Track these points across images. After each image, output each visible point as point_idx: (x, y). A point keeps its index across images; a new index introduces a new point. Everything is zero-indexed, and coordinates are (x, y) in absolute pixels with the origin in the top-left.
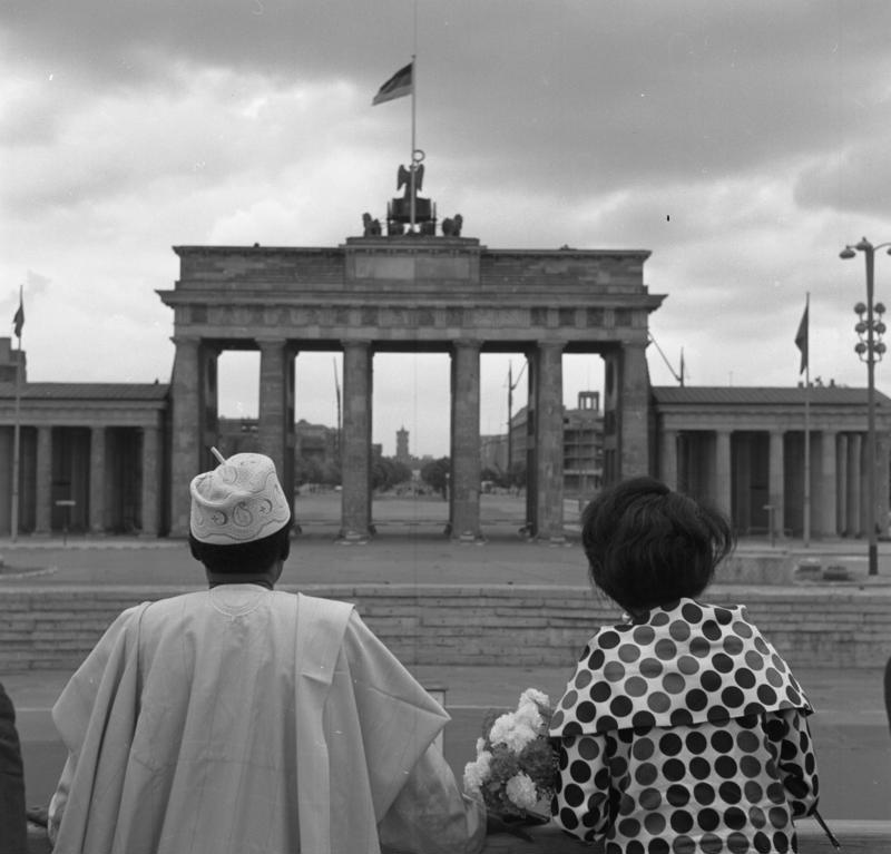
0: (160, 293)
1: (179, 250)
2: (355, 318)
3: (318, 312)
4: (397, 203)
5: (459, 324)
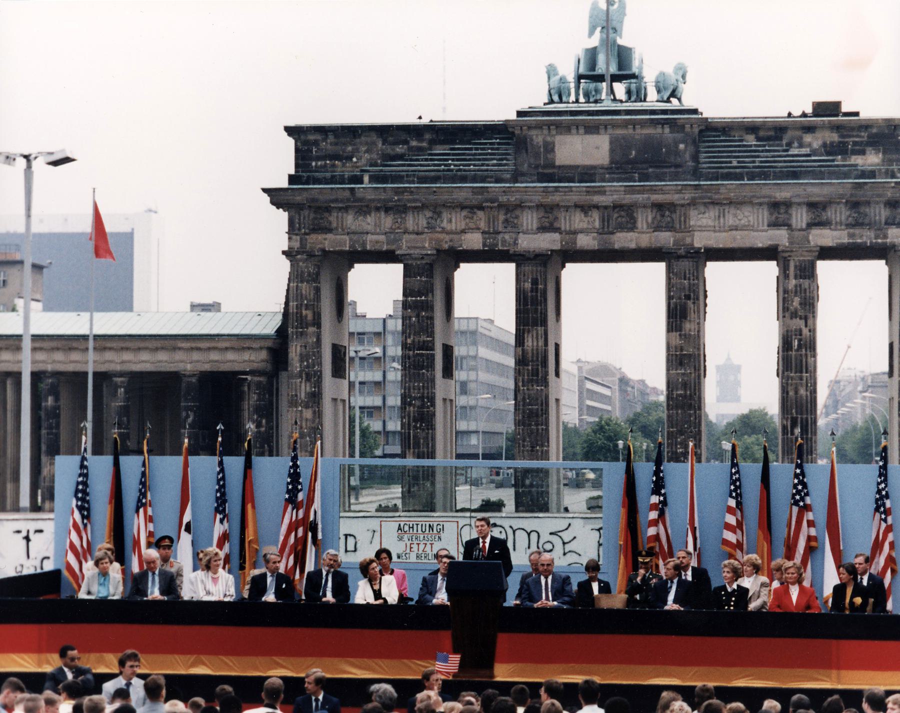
0: (265, 190)
1: (291, 131)
2: (529, 219)
3: (480, 214)
4: (592, 54)
5: (670, 228)
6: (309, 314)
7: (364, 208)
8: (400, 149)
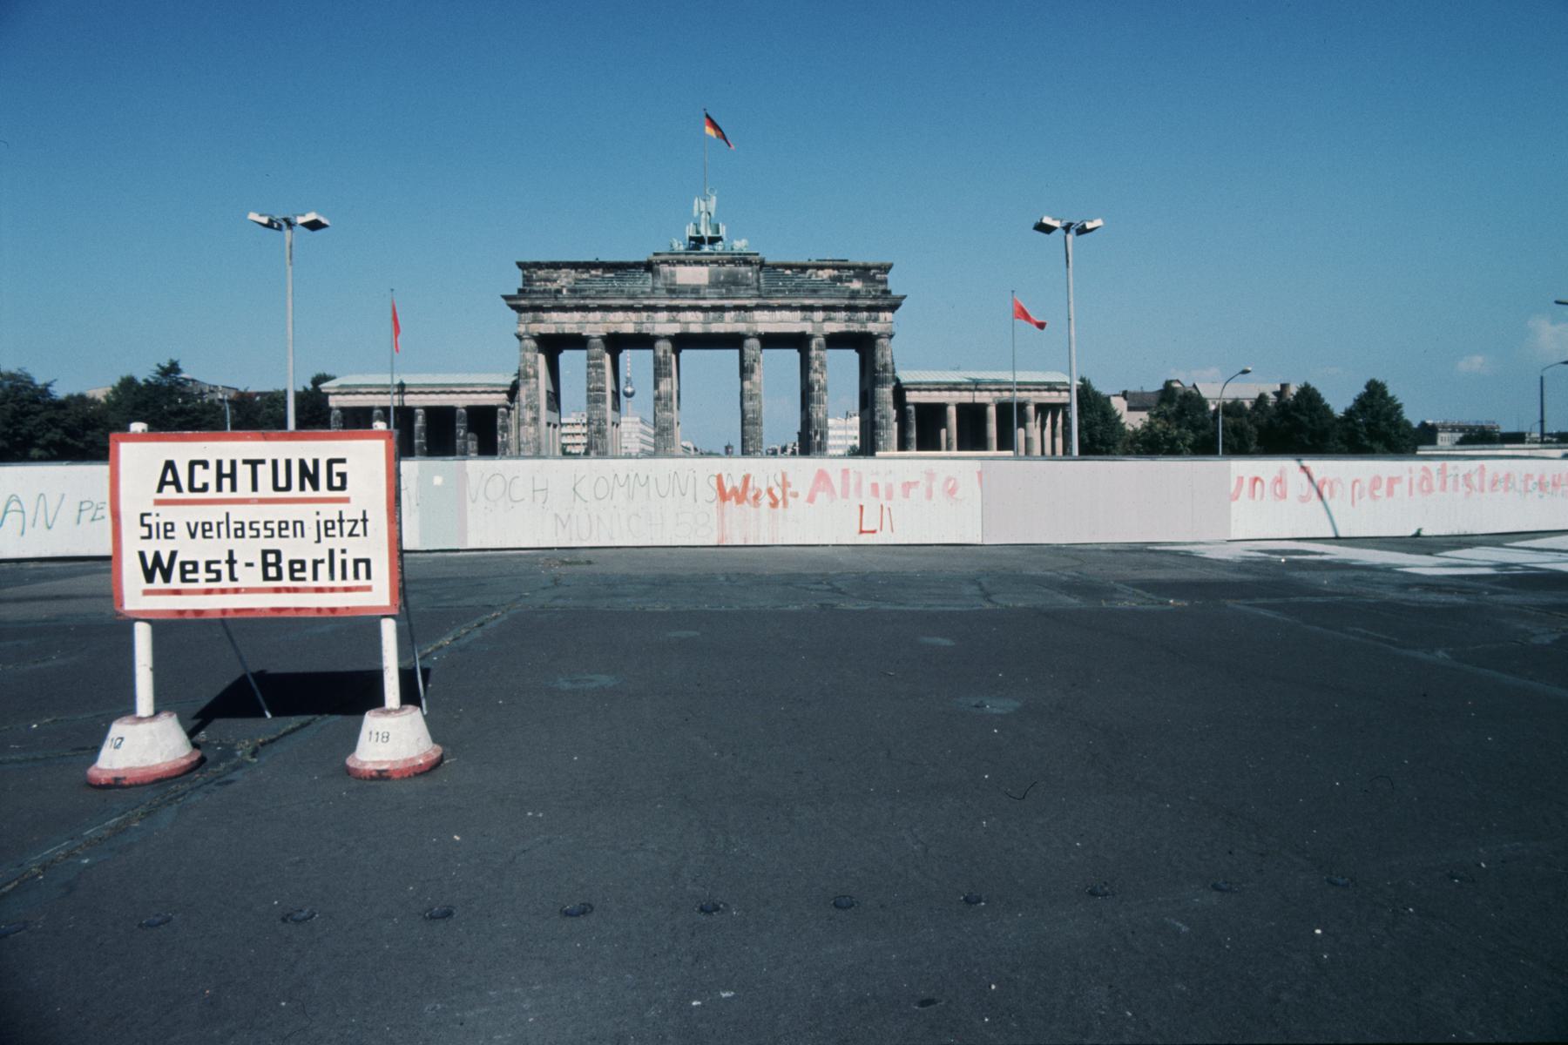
1: (521, 265)
6: (531, 371)
7: (564, 309)
8: (585, 276)
